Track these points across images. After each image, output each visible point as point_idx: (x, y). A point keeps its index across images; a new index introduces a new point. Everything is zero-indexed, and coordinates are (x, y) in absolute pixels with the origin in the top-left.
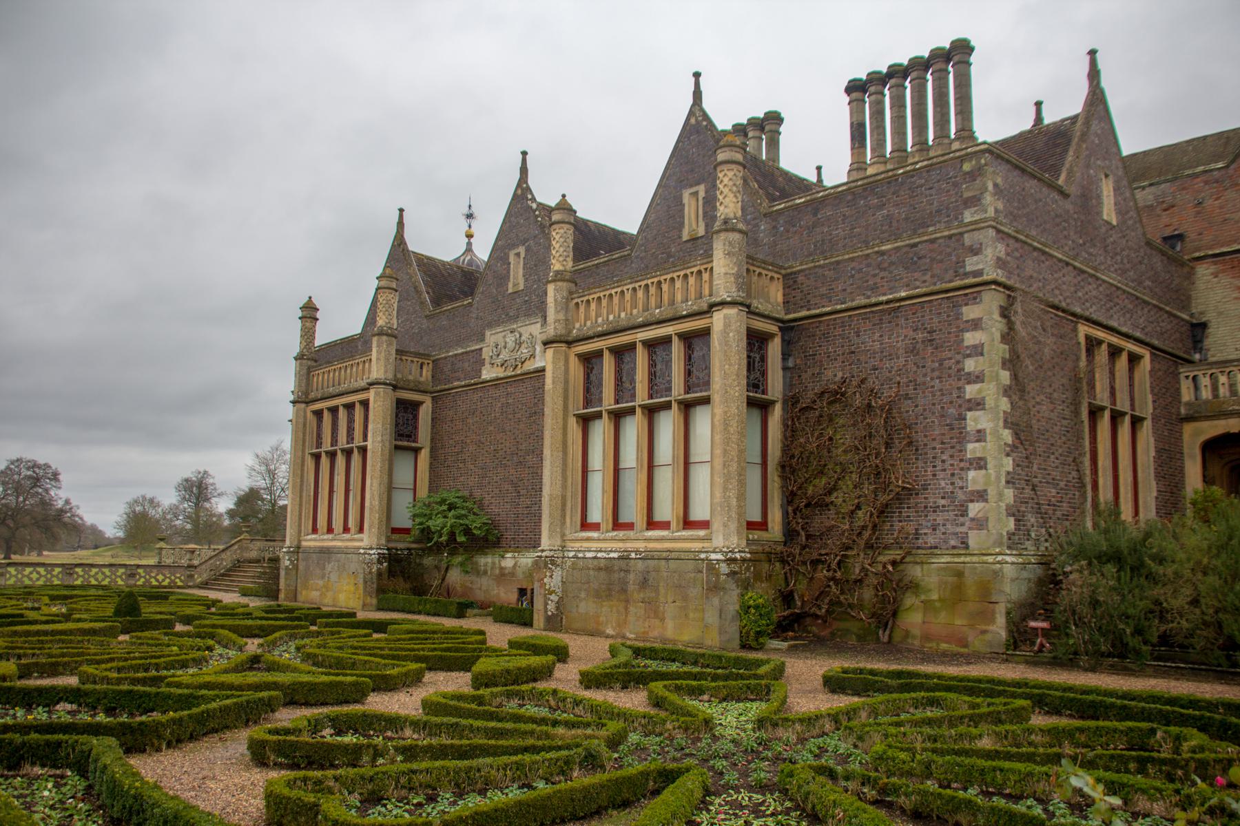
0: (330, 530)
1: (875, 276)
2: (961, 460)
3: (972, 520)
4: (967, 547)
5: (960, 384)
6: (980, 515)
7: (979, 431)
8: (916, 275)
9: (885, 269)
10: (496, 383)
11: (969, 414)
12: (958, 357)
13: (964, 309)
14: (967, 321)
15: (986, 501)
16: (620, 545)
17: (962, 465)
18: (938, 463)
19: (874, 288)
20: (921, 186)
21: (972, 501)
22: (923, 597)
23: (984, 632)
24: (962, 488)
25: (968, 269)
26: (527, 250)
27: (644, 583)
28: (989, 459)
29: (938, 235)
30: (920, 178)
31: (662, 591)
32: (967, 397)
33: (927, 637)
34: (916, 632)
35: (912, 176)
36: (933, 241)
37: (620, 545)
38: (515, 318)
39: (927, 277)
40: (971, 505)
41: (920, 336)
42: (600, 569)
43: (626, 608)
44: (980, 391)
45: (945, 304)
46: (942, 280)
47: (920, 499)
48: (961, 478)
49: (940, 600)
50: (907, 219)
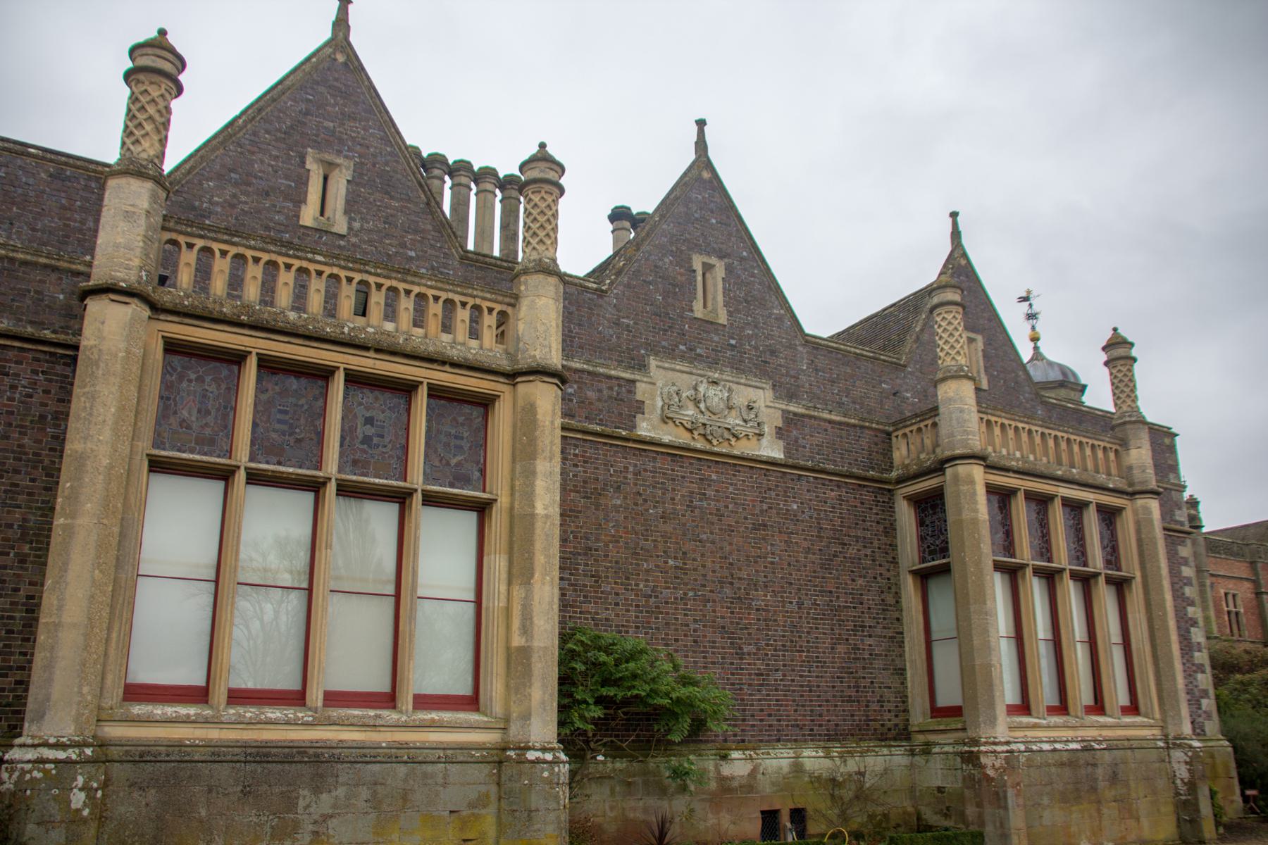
0: (1062, 707)
10: (676, 453)
16: (1069, 734)
26: (729, 269)
27: (1114, 779)
31: (1132, 784)
37: (1069, 734)
38: (713, 363)
42: (1062, 764)
43: (1099, 811)
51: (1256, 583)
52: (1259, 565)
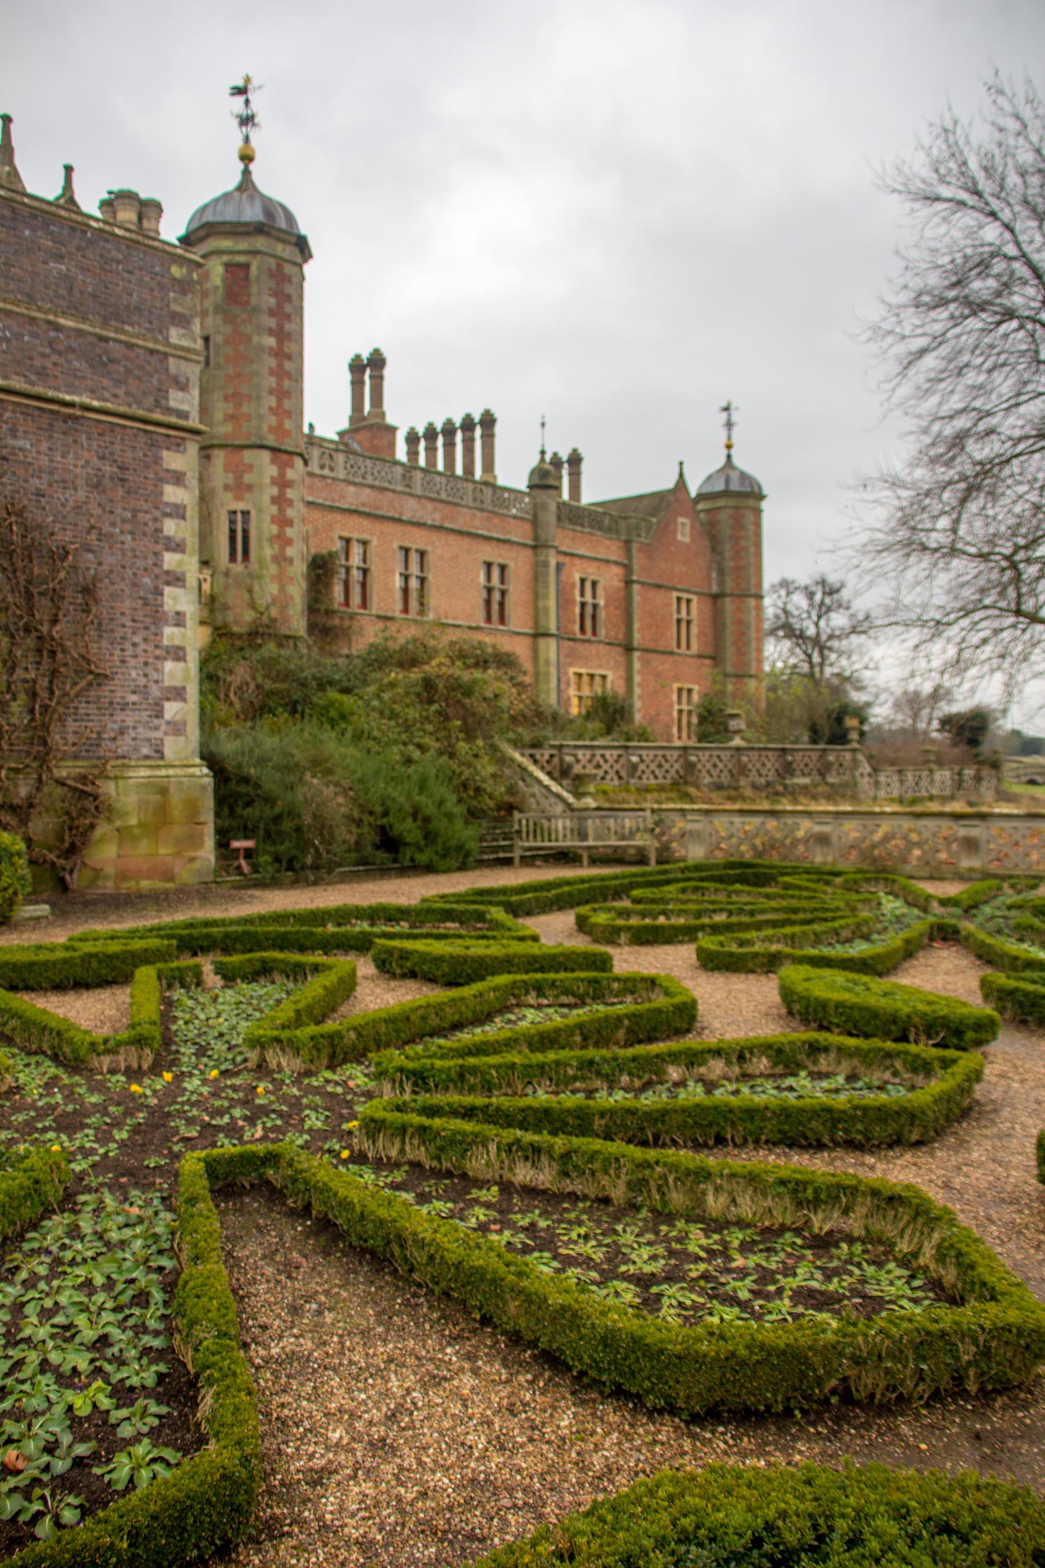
1: (44, 355)
2: (157, 647)
3: (169, 723)
4: (162, 757)
5: (159, 548)
6: (178, 718)
7: (178, 614)
8: (106, 382)
9: (60, 354)
11: (168, 590)
12: (157, 513)
13: (165, 454)
14: (168, 471)
15: (184, 700)
17: (158, 652)
18: (127, 645)
19: (42, 373)
20: (118, 262)
21: (168, 699)
22: (118, 823)
23: (192, 860)
24: (156, 682)
25: (172, 404)
28: (189, 650)
29: (140, 342)
30: (119, 250)
32: (166, 567)
33: (123, 876)
34: (110, 870)
35: (107, 241)
36: (130, 346)
39: (121, 392)
40: (168, 705)
41: (108, 469)
44: (180, 563)
45: (142, 438)
46: (139, 404)
47: (105, 691)
48: (156, 670)
49: (140, 825)
50: (94, 296)
51: (628, 568)
52: (635, 546)
